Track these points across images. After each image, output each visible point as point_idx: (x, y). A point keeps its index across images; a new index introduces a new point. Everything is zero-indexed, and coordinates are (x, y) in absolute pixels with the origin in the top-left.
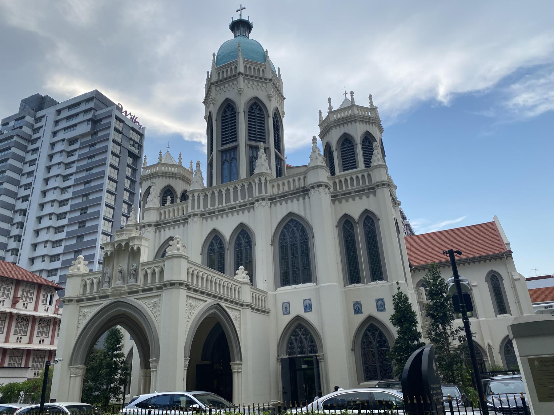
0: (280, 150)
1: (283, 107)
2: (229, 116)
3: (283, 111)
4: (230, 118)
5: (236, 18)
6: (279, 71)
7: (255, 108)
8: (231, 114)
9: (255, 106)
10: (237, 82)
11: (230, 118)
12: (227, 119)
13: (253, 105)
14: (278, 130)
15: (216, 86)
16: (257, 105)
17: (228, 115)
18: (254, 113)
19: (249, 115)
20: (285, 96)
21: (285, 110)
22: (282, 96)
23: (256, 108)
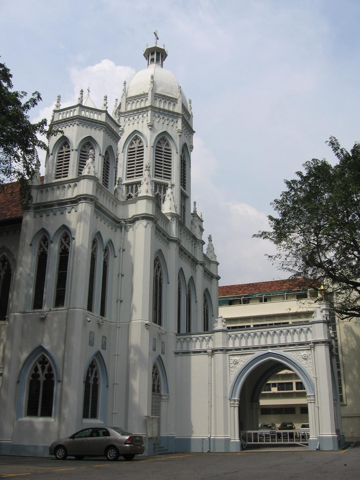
0: (185, 186)
1: (191, 141)
2: (136, 149)
3: (191, 144)
4: (138, 151)
5: (152, 45)
6: (190, 102)
7: (163, 142)
8: (138, 147)
9: (163, 141)
10: (147, 115)
11: (138, 151)
12: (134, 151)
13: (161, 140)
14: (185, 165)
15: (125, 117)
16: (165, 139)
17: (135, 148)
18: (161, 148)
19: (156, 150)
20: (194, 129)
21: (195, 144)
22: (192, 130)
23: (164, 143)
